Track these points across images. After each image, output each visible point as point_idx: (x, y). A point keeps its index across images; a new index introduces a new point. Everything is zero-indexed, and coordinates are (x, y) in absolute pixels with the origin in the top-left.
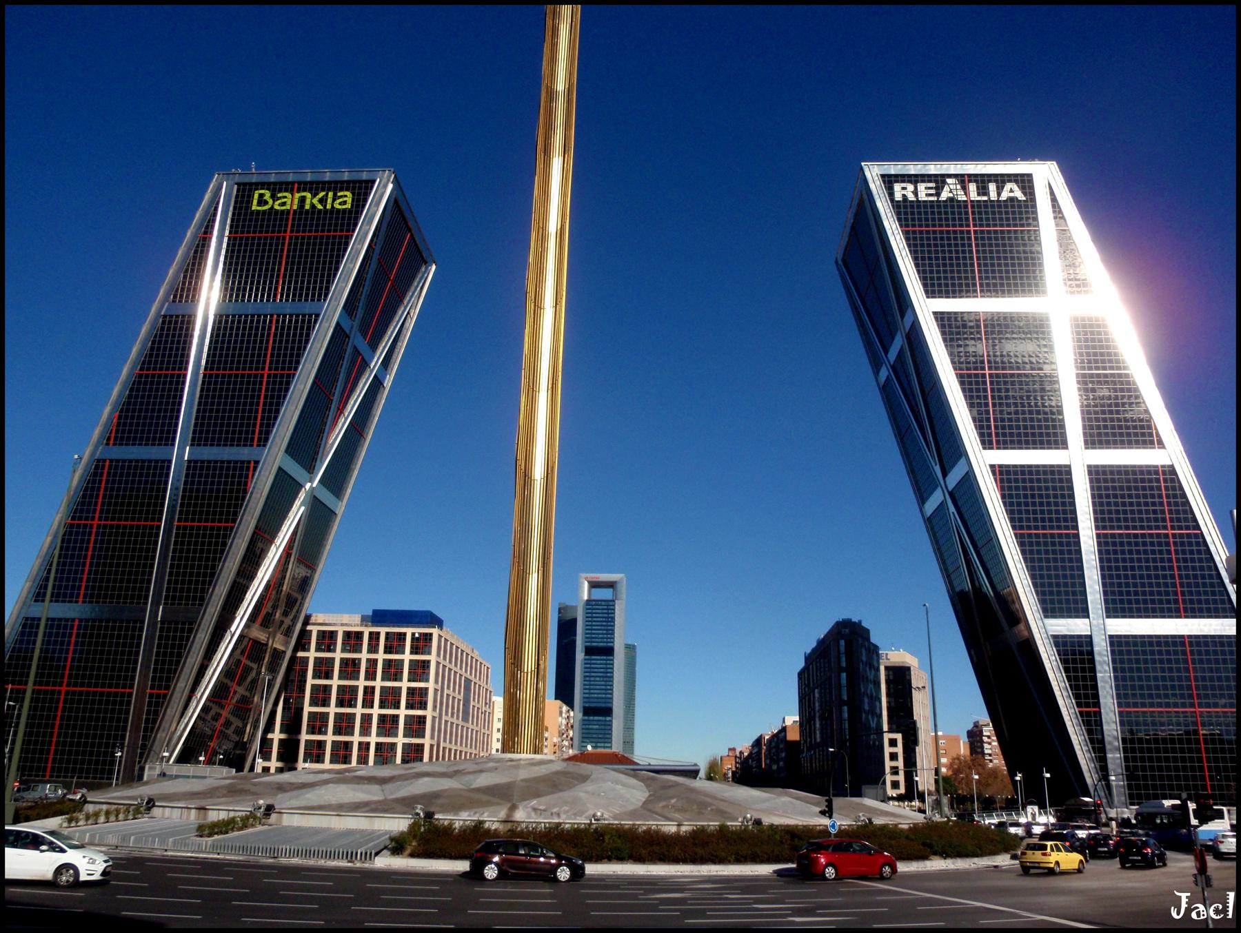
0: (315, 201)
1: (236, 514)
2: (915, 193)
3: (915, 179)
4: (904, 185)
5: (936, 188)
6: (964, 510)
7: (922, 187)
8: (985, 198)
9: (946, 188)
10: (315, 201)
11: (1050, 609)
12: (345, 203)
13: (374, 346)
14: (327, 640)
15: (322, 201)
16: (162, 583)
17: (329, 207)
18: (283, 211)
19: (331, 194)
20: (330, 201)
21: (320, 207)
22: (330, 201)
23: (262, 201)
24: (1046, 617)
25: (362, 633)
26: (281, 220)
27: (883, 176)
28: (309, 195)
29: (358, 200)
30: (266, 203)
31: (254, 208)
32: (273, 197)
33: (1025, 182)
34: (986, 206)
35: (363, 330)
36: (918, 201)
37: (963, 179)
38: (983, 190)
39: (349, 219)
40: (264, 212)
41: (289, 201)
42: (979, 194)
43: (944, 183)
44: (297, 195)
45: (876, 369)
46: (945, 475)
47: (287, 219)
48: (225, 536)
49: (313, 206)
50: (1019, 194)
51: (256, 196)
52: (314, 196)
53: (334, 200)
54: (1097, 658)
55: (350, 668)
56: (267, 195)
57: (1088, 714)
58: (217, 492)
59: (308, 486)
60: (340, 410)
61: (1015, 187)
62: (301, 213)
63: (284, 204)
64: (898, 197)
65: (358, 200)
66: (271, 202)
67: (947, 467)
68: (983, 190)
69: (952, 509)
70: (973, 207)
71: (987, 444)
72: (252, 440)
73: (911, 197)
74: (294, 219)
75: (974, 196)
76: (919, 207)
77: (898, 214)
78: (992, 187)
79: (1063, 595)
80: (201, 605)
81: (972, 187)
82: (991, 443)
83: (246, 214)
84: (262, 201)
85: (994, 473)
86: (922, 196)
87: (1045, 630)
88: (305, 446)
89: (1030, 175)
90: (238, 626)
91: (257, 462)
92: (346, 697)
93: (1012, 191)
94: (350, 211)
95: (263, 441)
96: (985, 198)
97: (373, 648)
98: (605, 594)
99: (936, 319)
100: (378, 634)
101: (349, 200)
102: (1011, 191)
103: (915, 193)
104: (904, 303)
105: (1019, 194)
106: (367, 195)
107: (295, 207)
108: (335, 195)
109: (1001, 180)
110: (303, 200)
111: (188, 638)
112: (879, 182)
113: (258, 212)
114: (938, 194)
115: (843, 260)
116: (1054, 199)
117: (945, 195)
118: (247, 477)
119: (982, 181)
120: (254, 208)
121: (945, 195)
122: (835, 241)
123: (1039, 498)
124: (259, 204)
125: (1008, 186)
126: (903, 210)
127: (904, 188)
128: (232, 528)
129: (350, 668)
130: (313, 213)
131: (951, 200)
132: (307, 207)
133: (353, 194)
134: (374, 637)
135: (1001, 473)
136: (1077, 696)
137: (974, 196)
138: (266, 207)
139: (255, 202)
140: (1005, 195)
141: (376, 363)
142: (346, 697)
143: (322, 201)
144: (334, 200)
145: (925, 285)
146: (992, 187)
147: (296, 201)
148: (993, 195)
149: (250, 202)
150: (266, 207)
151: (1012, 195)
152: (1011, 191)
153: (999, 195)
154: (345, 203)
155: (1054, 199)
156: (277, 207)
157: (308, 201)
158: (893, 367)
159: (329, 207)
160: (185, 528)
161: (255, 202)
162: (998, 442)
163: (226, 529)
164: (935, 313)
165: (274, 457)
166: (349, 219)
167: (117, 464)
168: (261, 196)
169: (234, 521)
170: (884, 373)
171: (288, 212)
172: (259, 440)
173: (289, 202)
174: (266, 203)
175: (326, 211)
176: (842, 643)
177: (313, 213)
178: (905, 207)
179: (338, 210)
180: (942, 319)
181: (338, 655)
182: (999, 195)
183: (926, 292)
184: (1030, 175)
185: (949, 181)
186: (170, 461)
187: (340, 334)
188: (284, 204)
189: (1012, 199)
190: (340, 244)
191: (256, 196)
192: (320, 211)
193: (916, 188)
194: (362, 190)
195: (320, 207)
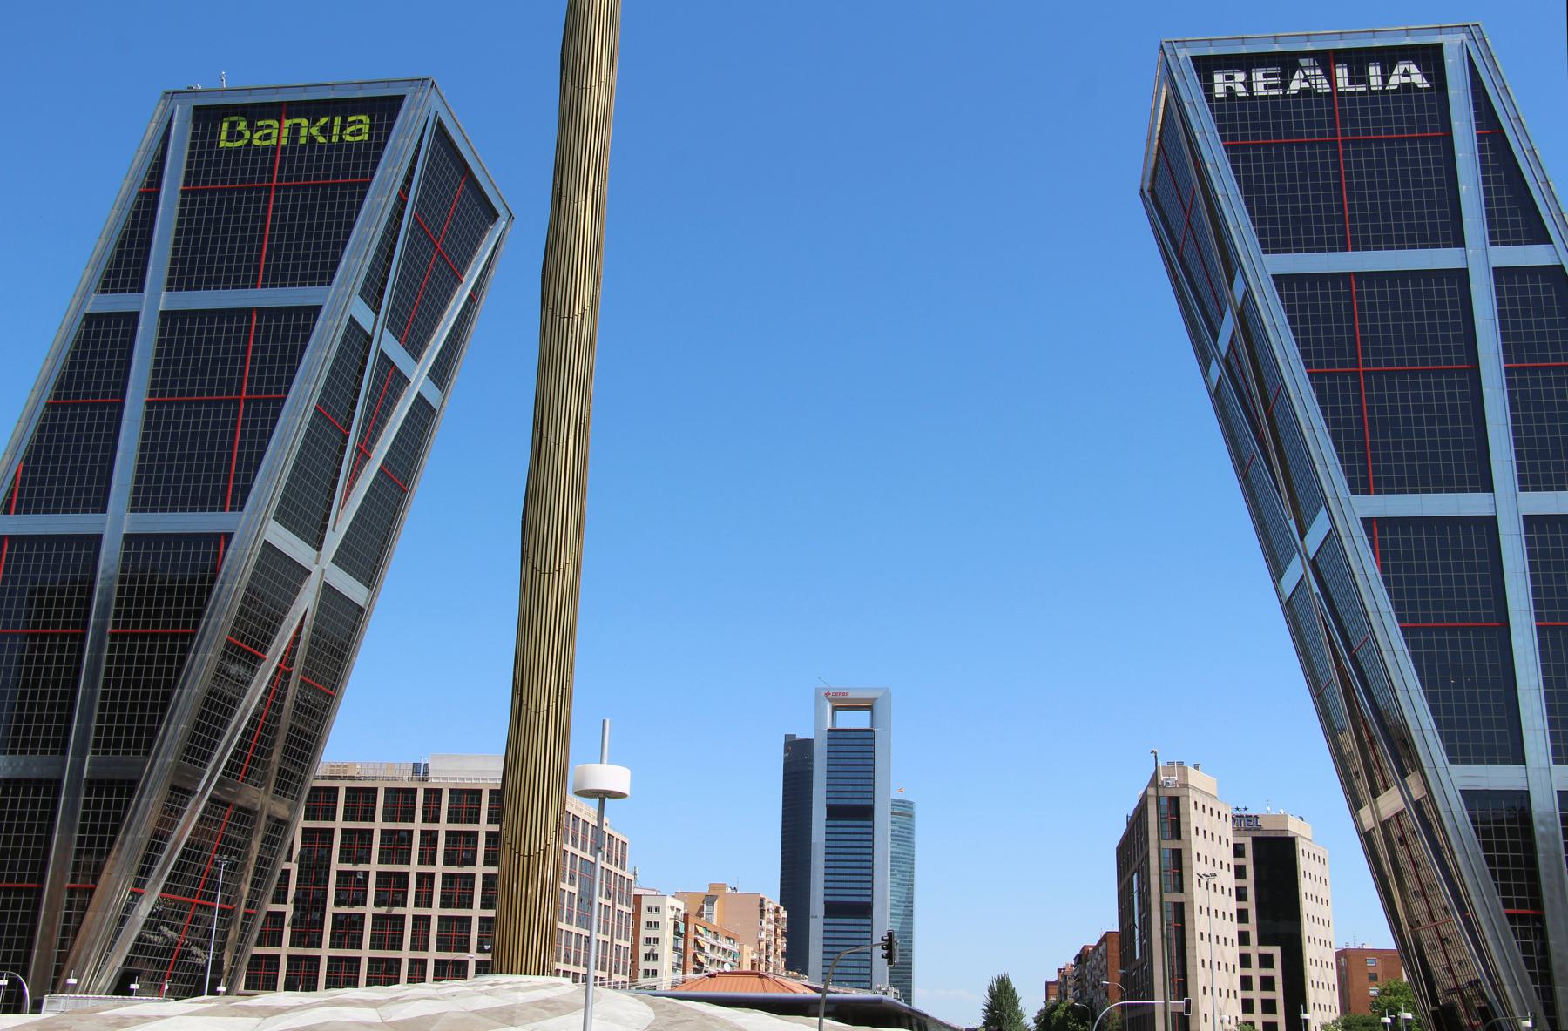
0: (314, 131)
1: (199, 614)
2: (1248, 84)
3: (1247, 63)
4: (1229, 72)
5: (1281, 75)
6: (1331, 589)
7: (1258, 76)
8: (1362, 88)
9: (1299, 75)
10: (314, 131)
11: (1458, 753)
12: (359, 132)
13: (416, 353)
14: (361, 801)
15: (323, 130)
16: (89, 721)
17: (335, 139)
18: (266, 149)
19: (337, 120)
20: (336, 130)
21: (321, 139)
22: (336, 130)
23: (234, 135)
24: (1452, 761)
26: (264, 161)
27: (1195, 59)
28: (304, 122)
29: (380, 127)
30: (241, 136)
31: (222, 144)
32: (250, 126)
33: (1430, 58)
34: (1363, 102)
35: (395, 325)
36: (1252, 97)
37: (1326, 60)
38: (1358, 76)
39: (366, 156)
40: (238, 150)
41: (275, 133)
42: (1351, 83)
43: (1297, 67)
44: (287, 123)
45: (1205, 366)
47: (273, 161)
48: (185, 649)
49: (312, 139)
50: (1418, 79)
51: (225, 126)
52: (313, 123)
53: (343, 129)
54: (1539, 829)
55: (396, 846)
56: (242, 126)
57: (1523, 919)
59: (315, 570)
60: (363, 454)
61: (1413, 69)
62: (293, 150)
63: (267, 137)
64: (1219, 90)
65: (380, 127)
66: (247, 135)
67: (1306, 521)
68: (1358, 76)
69: (1316, 589)
70: (1341, 102)
71: (1360, 484)
72: (224, 501)
73: (1240, 90)
74: (283, 160)
76: (1253, 107)
77: (1219, 119)
78: (1374, 70)
79: (1484, 728)
80: (147, 754)
81: (1341, 72)
83: (210, 154)
84: (234, 135)
86: (1259, 88)
88: (305, 513)
89: (1439, 47)
90: (207, 784)
91: (228, 537)
92: (392, 888)
93: (1410, 74)
94: (368, 145)
96: (1362, 88)
97: (431, 815)
98: (859, 720)
101: (366, 129)
102: (1406, 74)
103: (1248, 84)
104: (1231, 264)
105: (1418, 79)
106: (393, 119)
107: (284, 141)
108: (344, 120)
109: (1389, 57)
110: (296, 129)
111: (128, 803)
113: (229, 150)
114: (1285, 85)
115: (1152, 191)
117: (1295, 86)
119: (1357, 60)
120: (222, 144)
121: (1295, 86)
124: (230, 138)
125: (1400, 69)
126: (1227, 111)
127: (1232, 78)
128: (193, 636)
129: (396, 846)
130: (312, 149)
131: (1305, 93)
132: (303, 141)
133: (372, 120)
136: (1505, 890)
137: (1343, 84)
138: (240, 143)
139: (224, 136)
140: (1394, 81)
141: (418, 376)
142: (392, 888)
143: (323, 130)
144: (343, 129)
145: (1261, 233)
146: (1374, 70)
147: (285, 133)
148: (1375, 82)
149: (216, 136)
150: (240, 143)
151: (1406, 80)
152: (1406, 74)
153: (1385, 80)
154: (359, 132)
156: (256, 142)
157: (304, 132)
158: (1227, 361)
159: (335, 139)
160: (123, 637)
161: (224, 136)
162: (1377, 481)
163: (184, 636)
165: (259, 526)
166: (366, 156)
168: (233, 125)
169: (196, 625)
170: (1215, 371)
171: (274, 149)
172: (234, 501)
173: (275, 133)
174: (241, 136)
175: (330, 146)
176: (1165, 802)
177: (312, 149)
178: (1231, 108)
179: (349, 144)
180: (1289, 288)
181: (378, 825)
182: (1385, 80)
183: (1263, 243)
184: (1439, 47)
185: (1303, 62)
187: (357, 340)
188: (267, 137)
189: (1405, 88)
190: (352, 196)
191: (225, 126)
192: (321, 146)
193: (1249, 77)
194: (384, 109)
195: (321, 139)
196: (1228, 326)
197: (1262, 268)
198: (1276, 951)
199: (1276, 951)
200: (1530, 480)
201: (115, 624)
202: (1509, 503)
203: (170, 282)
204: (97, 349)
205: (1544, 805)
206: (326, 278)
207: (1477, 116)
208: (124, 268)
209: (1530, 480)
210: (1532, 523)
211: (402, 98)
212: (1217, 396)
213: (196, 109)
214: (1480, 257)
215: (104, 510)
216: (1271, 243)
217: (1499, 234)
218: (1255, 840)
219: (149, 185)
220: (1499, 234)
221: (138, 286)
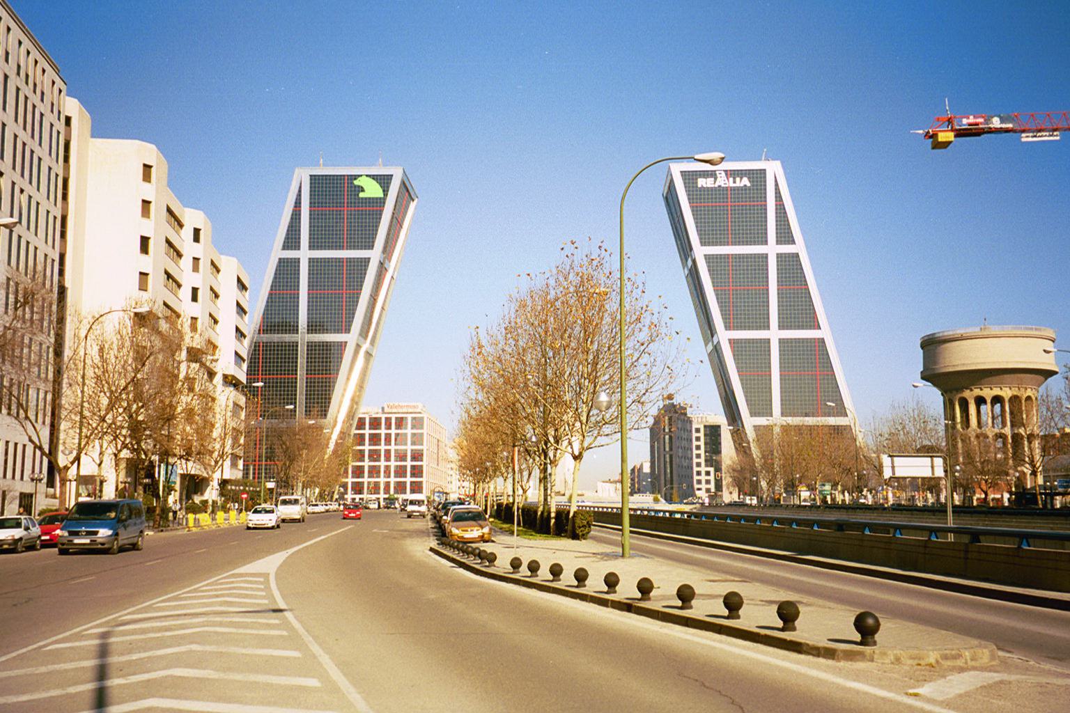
11: (753, 414)
25: (381, 418)
46: (712, 337)
58: (325, 362)
71: (728, 327)
75: (732, 185)
79: (761, 407)
82: (730, 327)
85: (730, 343)
87: (750, 422)
95: (348, 331)
99: (706, 259)
100: (390, 418)
112: (679, 174)
116: (777, 184)
117: (716, 186)
118: (342, 350)
122: (662, 189)
123: (752, 355)
131: (720, 186)
134: (388, 420)
135: (732, 342)
155: (777, 184)
164: (705, 255)
167: (268, 346)
170: (687, 272)
186: (297, 343)
196: (690, 263)
197: (700, 252)
198: (712, 470)
199: (712, 470)
200: (782, 326)
201: (307, 374)
202: (774, 334)
203: (310, 246)
204: (287, 270)
205: (777, 430)
206: (371, 247)
207: (776, 197)
208: (292, 241)
209: (782, 326)
210: (782, 341)
211: (392, 176)
212: (687, 277)
213: (311, 176)
214: (772, 249)
215: (297, 333)
216: (703, 243)
217: (779, 242)
218: (705, 426)
219: (295, 207)
220: (779, 242)
221: (297, 247)
